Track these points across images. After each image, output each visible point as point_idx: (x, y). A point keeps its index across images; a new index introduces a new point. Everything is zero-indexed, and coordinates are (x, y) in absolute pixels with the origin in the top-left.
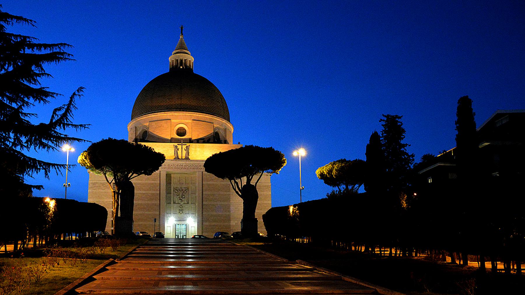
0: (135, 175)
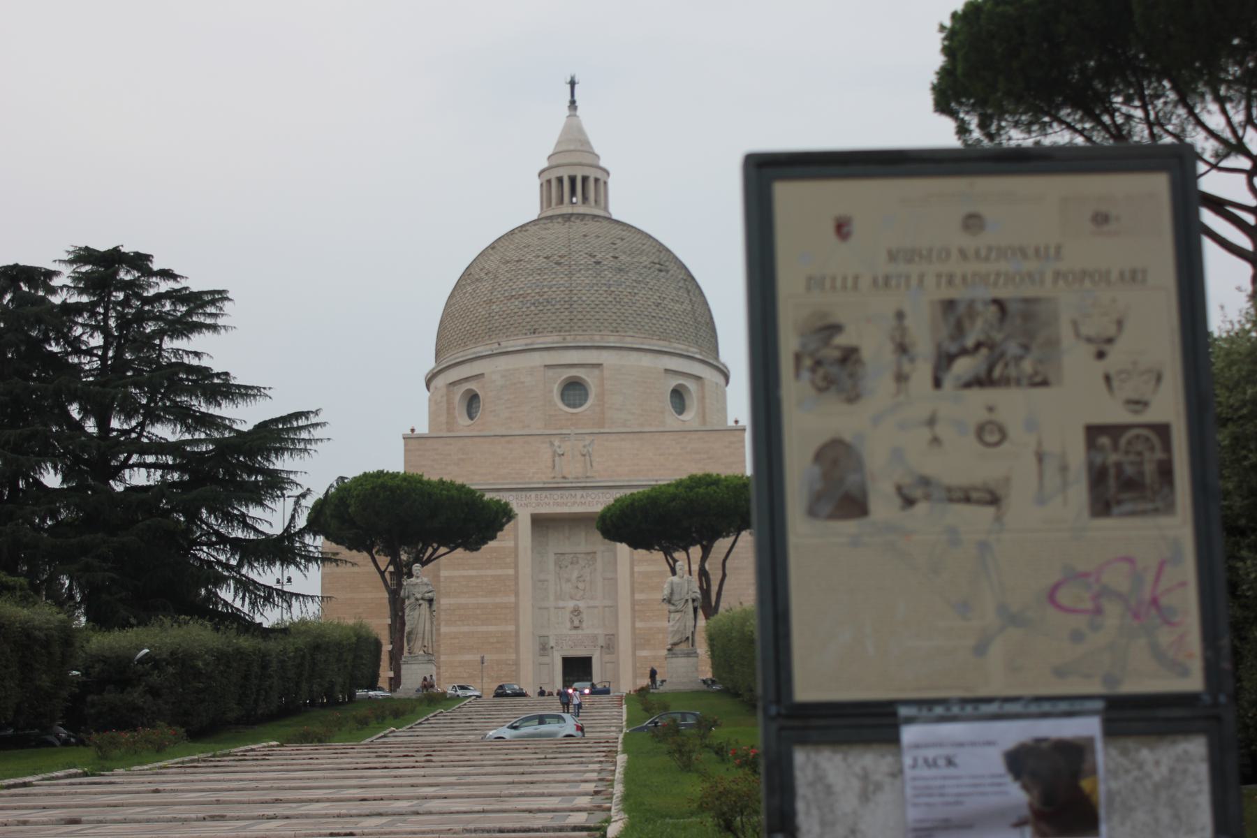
0: (443, 550)
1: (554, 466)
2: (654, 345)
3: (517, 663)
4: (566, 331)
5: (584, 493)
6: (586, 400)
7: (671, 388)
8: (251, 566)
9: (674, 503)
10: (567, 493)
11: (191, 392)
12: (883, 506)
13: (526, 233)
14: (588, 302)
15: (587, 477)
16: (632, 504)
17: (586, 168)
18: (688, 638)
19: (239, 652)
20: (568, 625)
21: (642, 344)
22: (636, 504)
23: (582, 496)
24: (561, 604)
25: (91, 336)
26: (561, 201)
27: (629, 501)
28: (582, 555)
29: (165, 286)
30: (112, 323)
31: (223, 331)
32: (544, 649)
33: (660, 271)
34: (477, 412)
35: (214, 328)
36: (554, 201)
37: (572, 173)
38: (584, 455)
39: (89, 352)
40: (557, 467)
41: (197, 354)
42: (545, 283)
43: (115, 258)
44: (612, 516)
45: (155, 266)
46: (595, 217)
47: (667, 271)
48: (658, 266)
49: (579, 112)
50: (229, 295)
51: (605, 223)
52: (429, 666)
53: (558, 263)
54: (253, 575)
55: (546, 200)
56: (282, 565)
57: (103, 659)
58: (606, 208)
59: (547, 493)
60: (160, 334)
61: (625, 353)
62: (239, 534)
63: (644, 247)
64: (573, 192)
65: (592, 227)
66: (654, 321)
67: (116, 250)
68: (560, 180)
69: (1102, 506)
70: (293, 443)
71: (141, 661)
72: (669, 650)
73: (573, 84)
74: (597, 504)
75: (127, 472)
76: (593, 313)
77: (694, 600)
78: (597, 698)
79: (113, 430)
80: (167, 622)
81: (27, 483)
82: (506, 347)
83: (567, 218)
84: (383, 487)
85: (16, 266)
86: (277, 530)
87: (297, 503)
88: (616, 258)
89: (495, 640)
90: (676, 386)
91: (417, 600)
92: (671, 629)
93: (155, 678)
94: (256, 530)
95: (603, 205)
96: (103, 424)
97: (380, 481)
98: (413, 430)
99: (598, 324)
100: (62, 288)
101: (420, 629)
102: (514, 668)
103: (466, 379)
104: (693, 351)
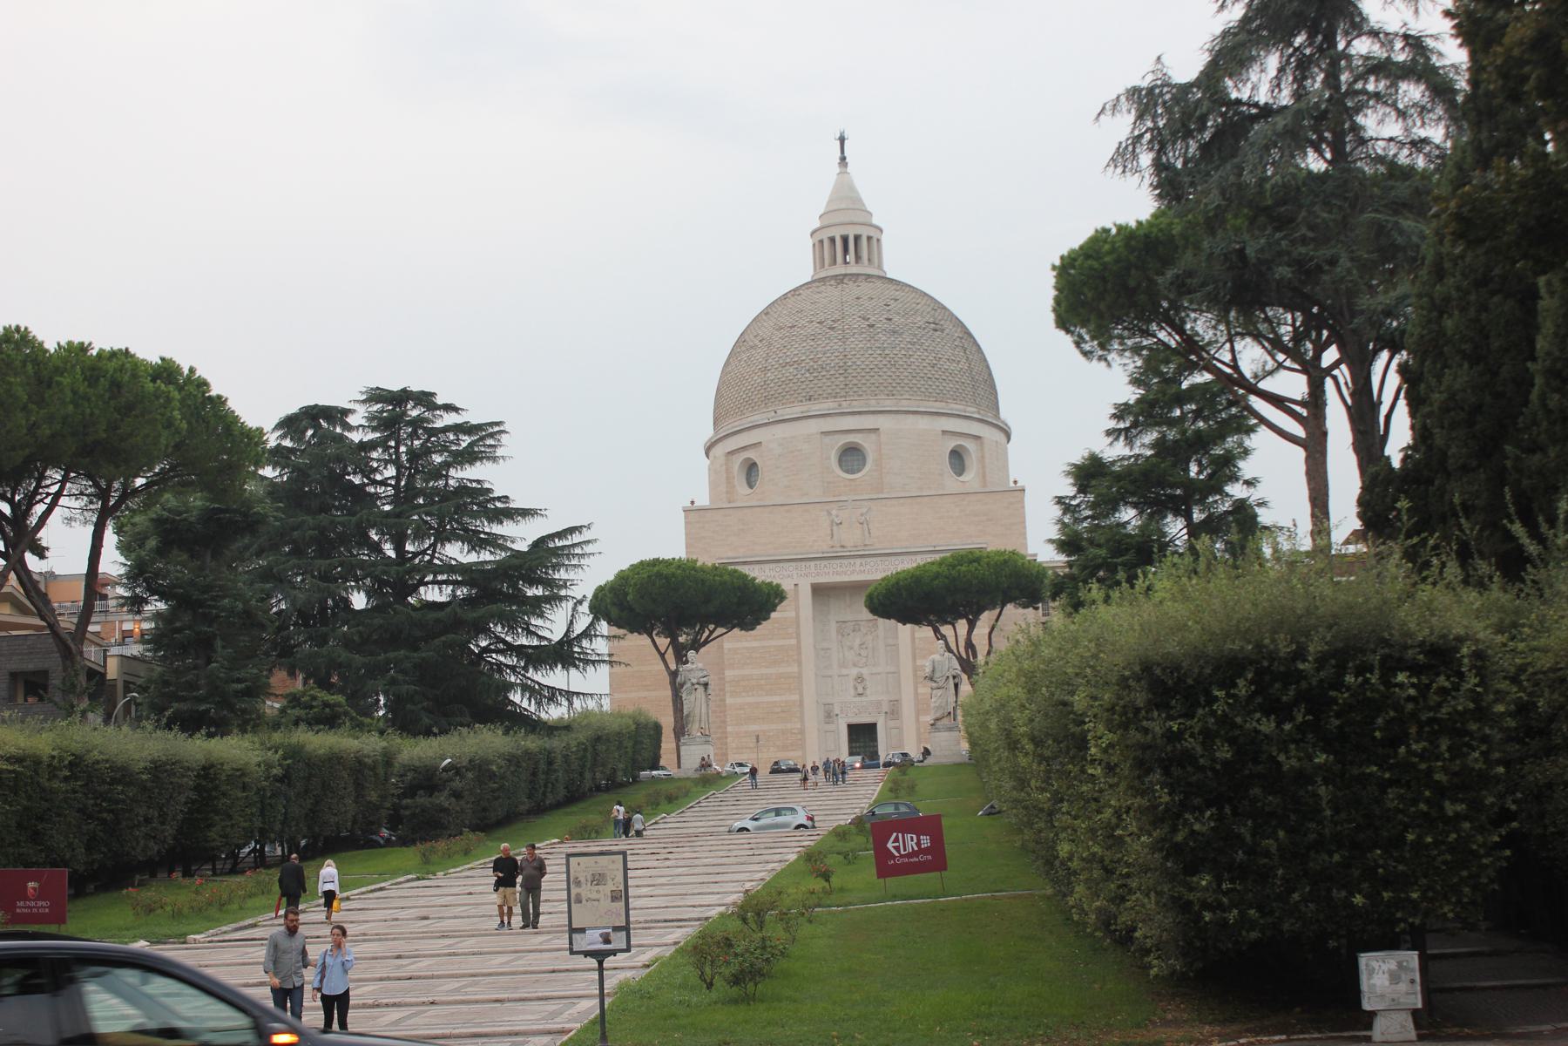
0: (720, 630)
1: (832, 535)
2: (932, 407)
3: (802, 732)
4: (841, 397)
5: (863, 560)
6: (864, 465)
7: (950, 449)
8: (536, 669)
9: (937, 582)
10: (845, 562)
11: (475, 515)
12: (584, 902)
13: (799, 298)
14: (863, 367)
15: (866, 545)
16: (897, 583)
17: (858, 227)
18: (950, 713)
19: (527, 754)
20: (852, 692)
21: (919, 407)
22: (901, 583)
23: (861, 564)
24: (844, 671)
25: (385, 468)
26: (834, 262)
27: (894, 581)
28: (863, 623)
29: (449, 419)
30: (404, 458)
31: (501, 461)
32: (829, 716)
33: (936, 330)
34: (756, 481)
35: (494, 459)
36: (827, 262)
37: (844, 233)
38: (862, 524)
39: (383, 483)
40: (835, 537)
41: (478, 482)
42: (819, 349)
43: (403, 396)
44: (878, 596)
45: (440, 401)
46: (869, 276)
47: (943, 331)
48: (933, 325)
49: (849, 170)
50: (505, 427)
51: (879, 283)
52: (706, 746)
53: (832, 328)
54: (538, 677)
55: (819, 262)
56: (563, 667)
57: (415, 770)
58: (880, 267)
59: (826, 562)
60: (447, 465)
61: (903, 416)
62: (524, 641)
63: (919, 306)
64: (846, 250)
65: (865, 288)
66: (930, 383)
67: (404, 391)
68: (832, 240)
69: (613, 901)
70: (569, 559)
71: (445, 769)
72: (932, 725)
73: (842, 140)
74: (876, 572)
75: (422, 589)
76: (868, 378)
77: (954, 677)
78: (865, 772)
79: (409, 552)
80: (464, 730)
81: (333, 600)
82: (782, 415)
83: (840, 279)
84: (659, 575)
85: (316, 405)
86: (556, 636)
87: (574, 609)
88: (890, 320)
89: (779, 710)
90: (956, 446)
91: (693, 684)
92: (932, 705)
93: (457, 784)
94: (541, 638)
95: (876, 261)
96: (399, 548)
97: (656, 569)
98: (692, 503)
99: (873, 389)
100: (358, 427)
101: (697, 711)
102: (799, 737)
103: (744, 448)
104: (971, 411)
